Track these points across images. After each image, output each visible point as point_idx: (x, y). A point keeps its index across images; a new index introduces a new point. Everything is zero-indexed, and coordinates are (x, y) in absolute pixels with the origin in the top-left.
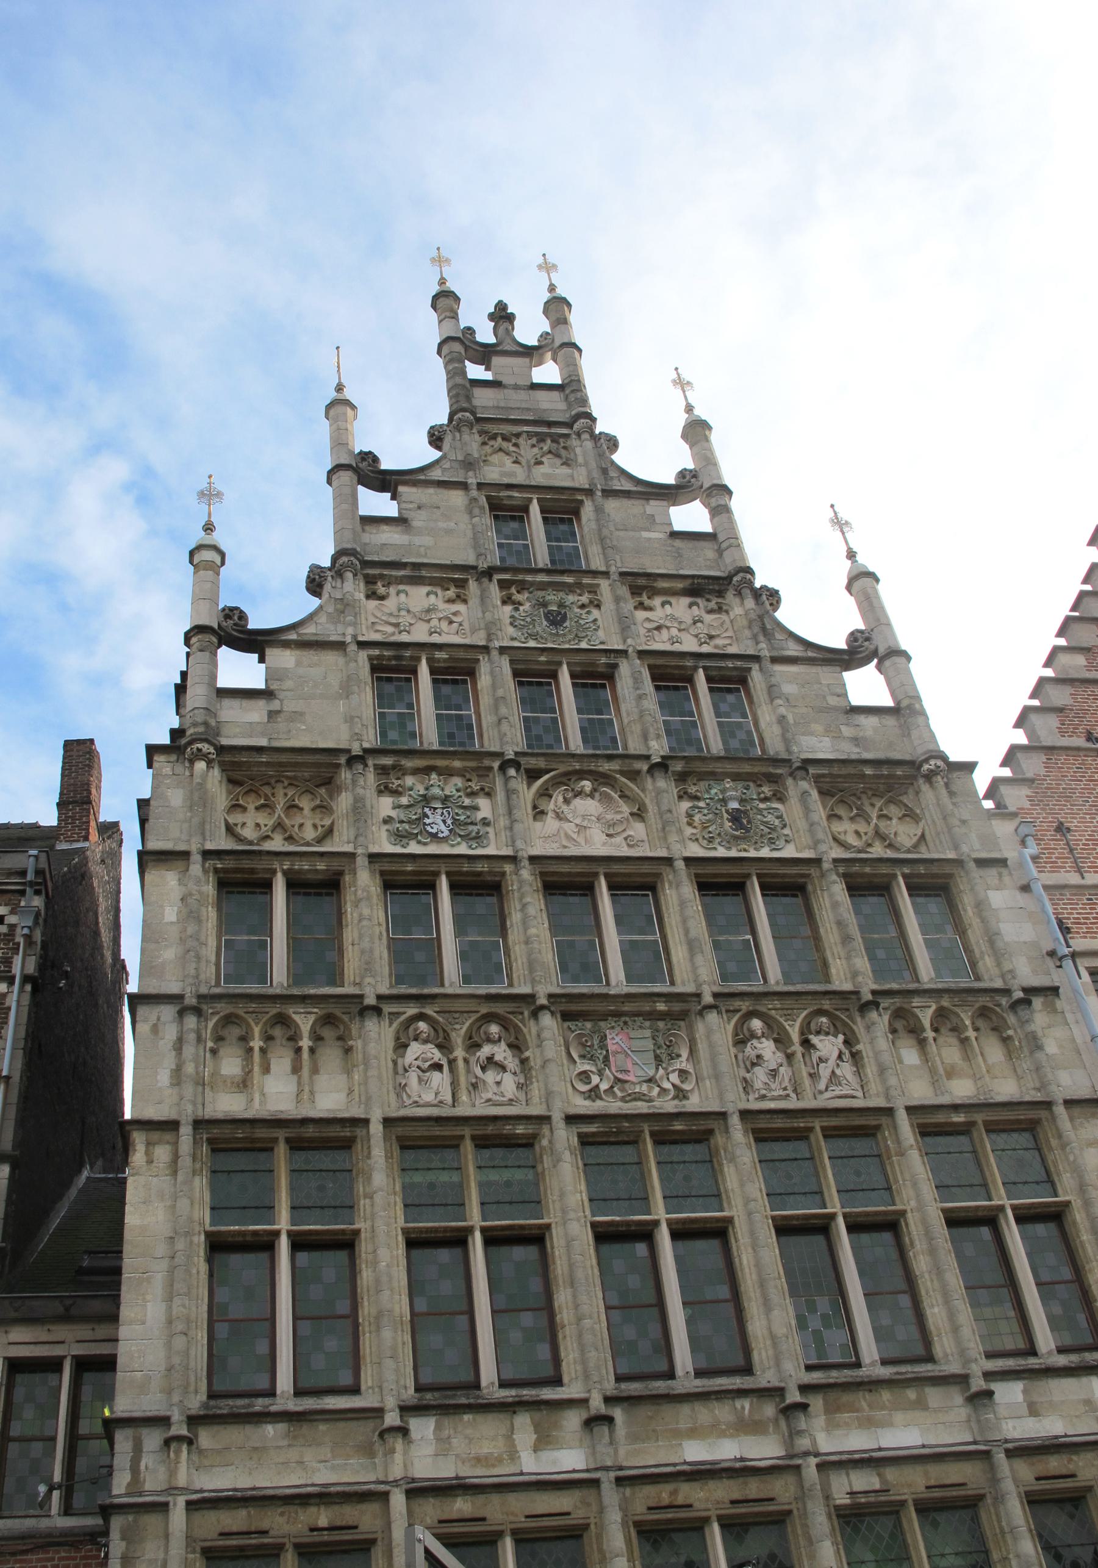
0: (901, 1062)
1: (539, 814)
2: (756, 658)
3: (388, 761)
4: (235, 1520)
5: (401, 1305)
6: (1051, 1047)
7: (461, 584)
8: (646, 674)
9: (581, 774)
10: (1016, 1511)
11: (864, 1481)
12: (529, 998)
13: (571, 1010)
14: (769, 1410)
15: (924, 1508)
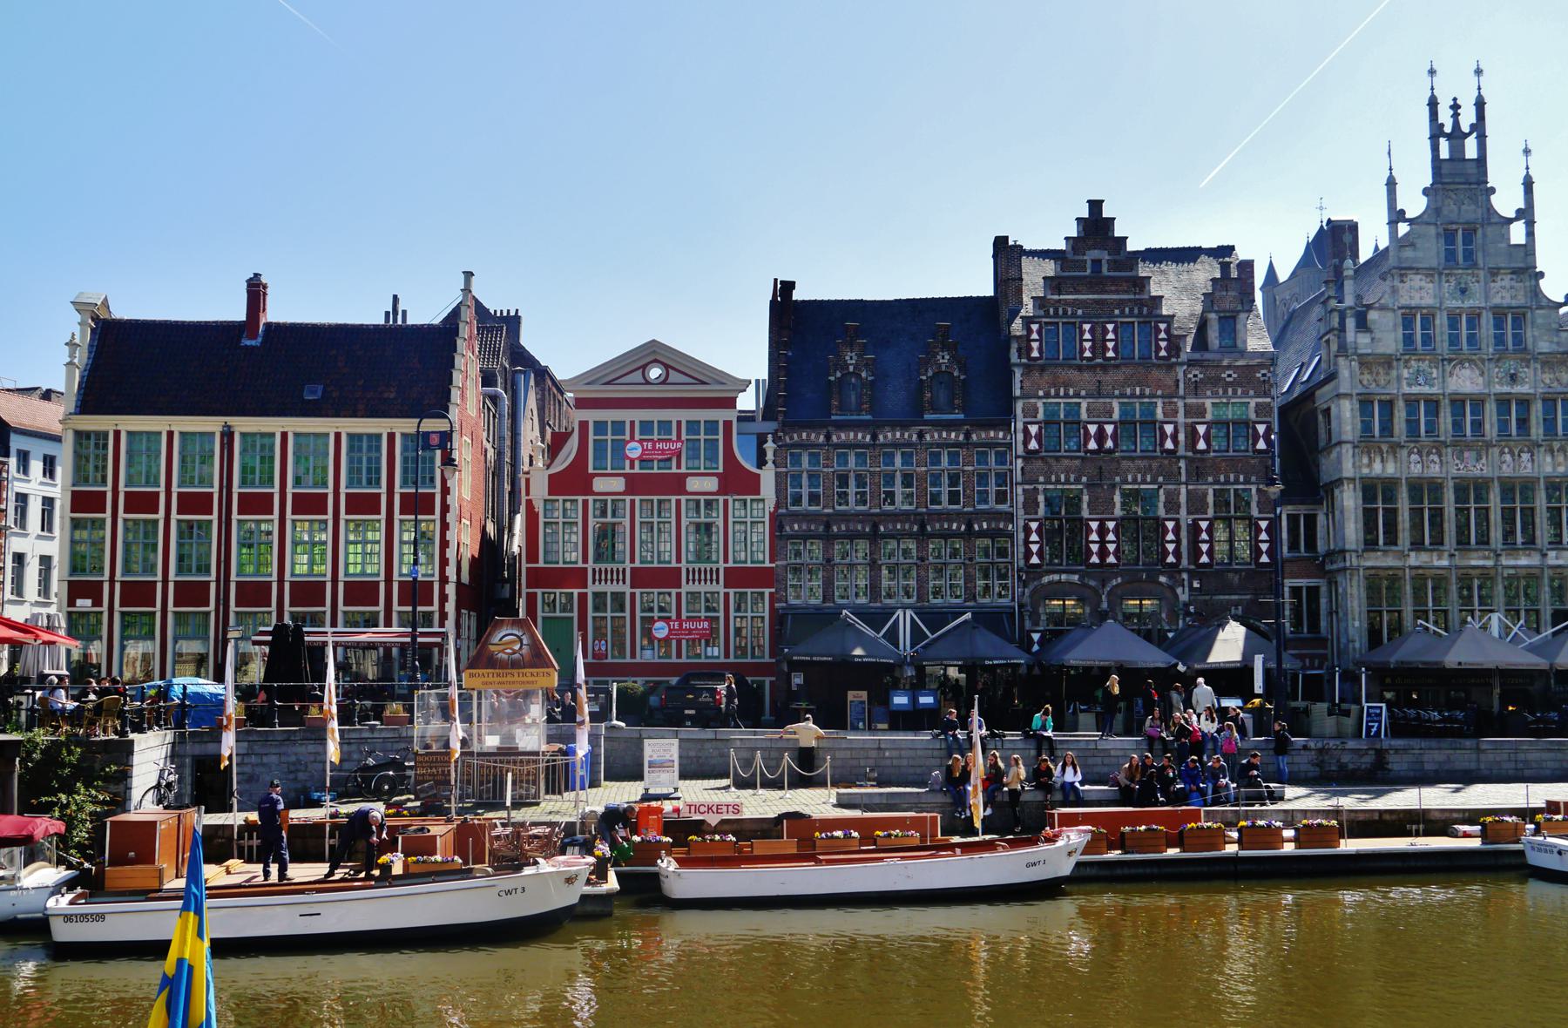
1: (1451, 374)
5: (1407, 525)
10: (1546, 581)
11: (1512, 571)
12: (1444, 443)
13: (1454, 444)
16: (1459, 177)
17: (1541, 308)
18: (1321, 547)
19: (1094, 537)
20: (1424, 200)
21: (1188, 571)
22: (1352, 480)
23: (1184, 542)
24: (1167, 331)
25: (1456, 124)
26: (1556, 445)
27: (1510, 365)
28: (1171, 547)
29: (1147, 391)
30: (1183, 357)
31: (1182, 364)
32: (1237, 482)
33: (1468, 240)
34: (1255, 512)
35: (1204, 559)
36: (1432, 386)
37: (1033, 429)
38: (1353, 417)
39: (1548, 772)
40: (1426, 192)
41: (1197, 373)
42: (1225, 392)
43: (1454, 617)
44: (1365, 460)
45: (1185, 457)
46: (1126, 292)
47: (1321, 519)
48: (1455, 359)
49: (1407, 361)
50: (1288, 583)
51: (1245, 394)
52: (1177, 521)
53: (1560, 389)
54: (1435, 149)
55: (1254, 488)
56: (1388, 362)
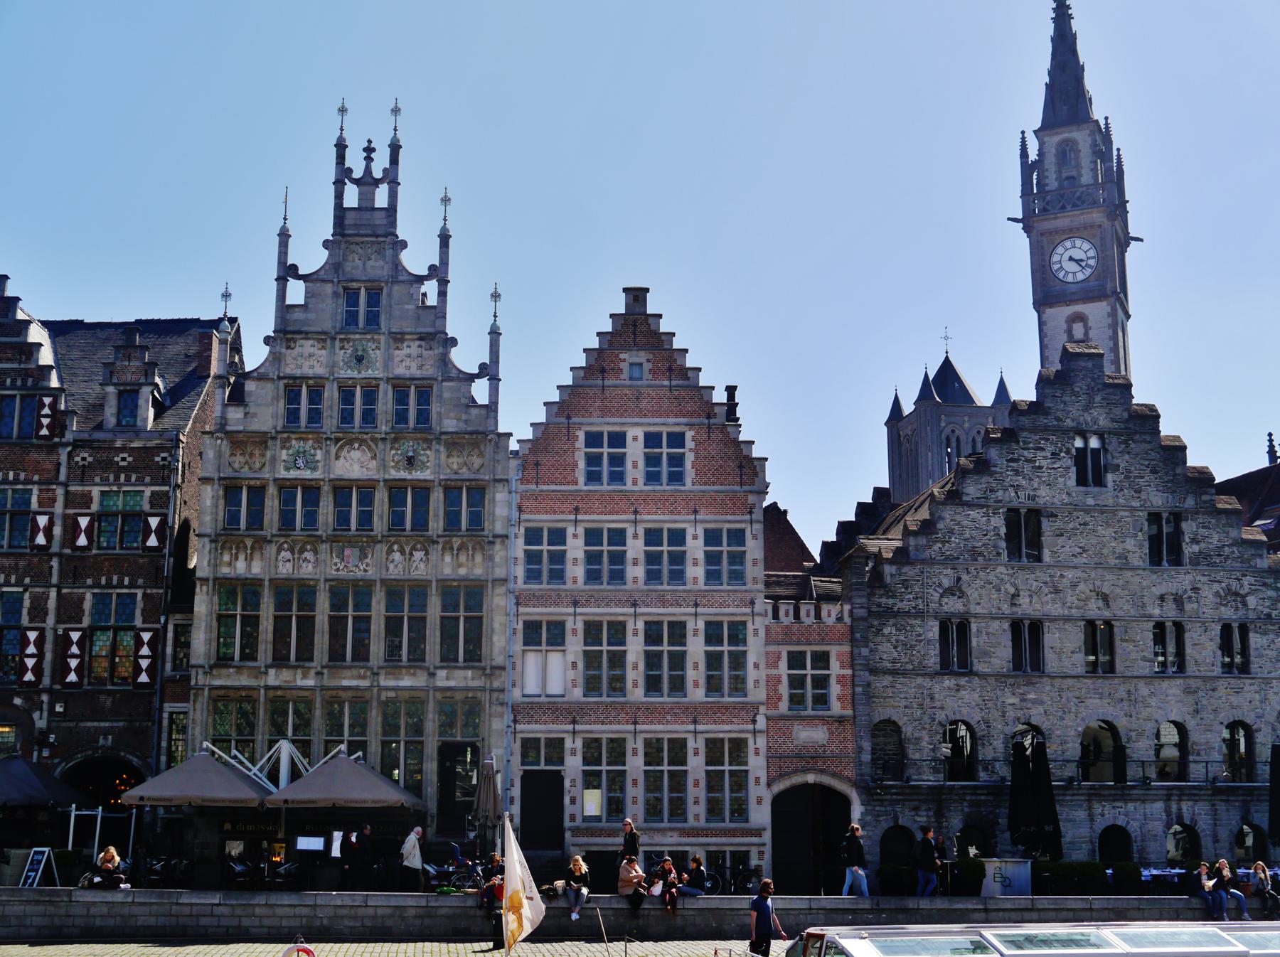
0: (443, 560)
1: (337, 458)
2: (436, 379)
3: (285, 435)
4: (222, 692)
5: (270, 637)
6: (497, 559)
7: (324, 341)
8: (390, 388)
9: (356, 439)
10: (431, 706)
11: (391, 694)
12: (320, 537)
13: (332, 540)
14: (369, 673)
15: (406, 702)
16: (364, 229)
17: (450, 379)
20: (325, 254)
21: (49, 691)
22: (207, 580)
23: (49, 656)
24: (53, 406)
25: (368, 170)
26: (456, 542)
27: (408, 447)
28: (30, 662)
29: (22, 476)
30: (69, 437)
31: (66, 445)
32: (121, 585)
33: (374, 298)
34: (138, 622)
35: (72, 677)
36: (314, 469)
38: (216, 506)
39: (33, 931)
40: (326, 244)
41: (84, 457)
42: (117, 478)
43: (317, 747)
44: (226, 558)
45: (60, 555)
46: (9, 360)
48: (345, 440)
49: (288, 440)
50: (168, 707)
51: (140, 481)
52: (42, 631)
53: (466, 476)
54: (339, 196)
55: (140, 593)
56: (262, 440)
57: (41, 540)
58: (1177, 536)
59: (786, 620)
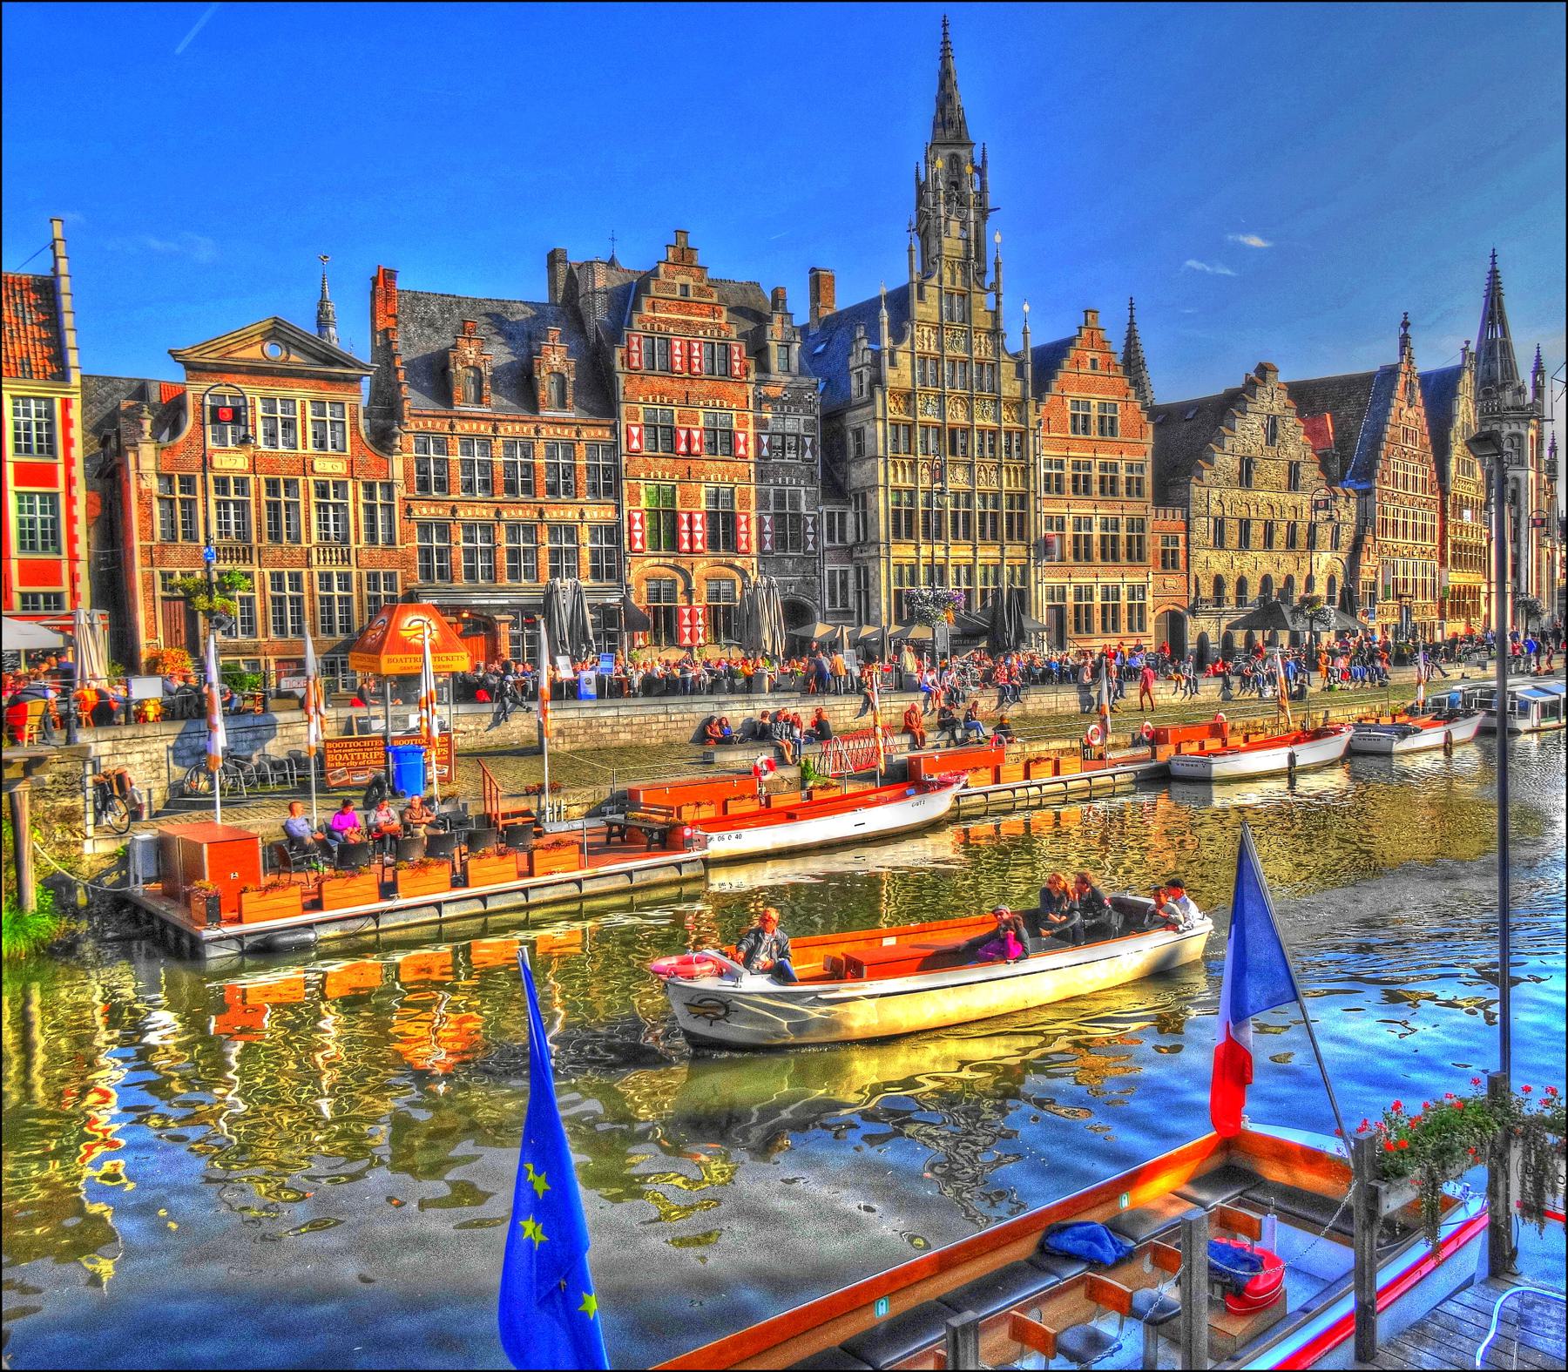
18: (850, 538)
19: (685, 527)
28: (743, 537)
32: (790, 484)
35: (768, 547)
37: (635, 431)
47: (850, 518)
50: (828, 568)
52: (747, 514)
57: (741, 451)
58: (1297, 472)
59: (1161, 518)
